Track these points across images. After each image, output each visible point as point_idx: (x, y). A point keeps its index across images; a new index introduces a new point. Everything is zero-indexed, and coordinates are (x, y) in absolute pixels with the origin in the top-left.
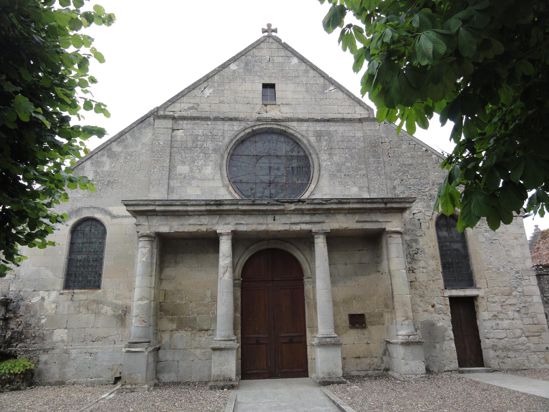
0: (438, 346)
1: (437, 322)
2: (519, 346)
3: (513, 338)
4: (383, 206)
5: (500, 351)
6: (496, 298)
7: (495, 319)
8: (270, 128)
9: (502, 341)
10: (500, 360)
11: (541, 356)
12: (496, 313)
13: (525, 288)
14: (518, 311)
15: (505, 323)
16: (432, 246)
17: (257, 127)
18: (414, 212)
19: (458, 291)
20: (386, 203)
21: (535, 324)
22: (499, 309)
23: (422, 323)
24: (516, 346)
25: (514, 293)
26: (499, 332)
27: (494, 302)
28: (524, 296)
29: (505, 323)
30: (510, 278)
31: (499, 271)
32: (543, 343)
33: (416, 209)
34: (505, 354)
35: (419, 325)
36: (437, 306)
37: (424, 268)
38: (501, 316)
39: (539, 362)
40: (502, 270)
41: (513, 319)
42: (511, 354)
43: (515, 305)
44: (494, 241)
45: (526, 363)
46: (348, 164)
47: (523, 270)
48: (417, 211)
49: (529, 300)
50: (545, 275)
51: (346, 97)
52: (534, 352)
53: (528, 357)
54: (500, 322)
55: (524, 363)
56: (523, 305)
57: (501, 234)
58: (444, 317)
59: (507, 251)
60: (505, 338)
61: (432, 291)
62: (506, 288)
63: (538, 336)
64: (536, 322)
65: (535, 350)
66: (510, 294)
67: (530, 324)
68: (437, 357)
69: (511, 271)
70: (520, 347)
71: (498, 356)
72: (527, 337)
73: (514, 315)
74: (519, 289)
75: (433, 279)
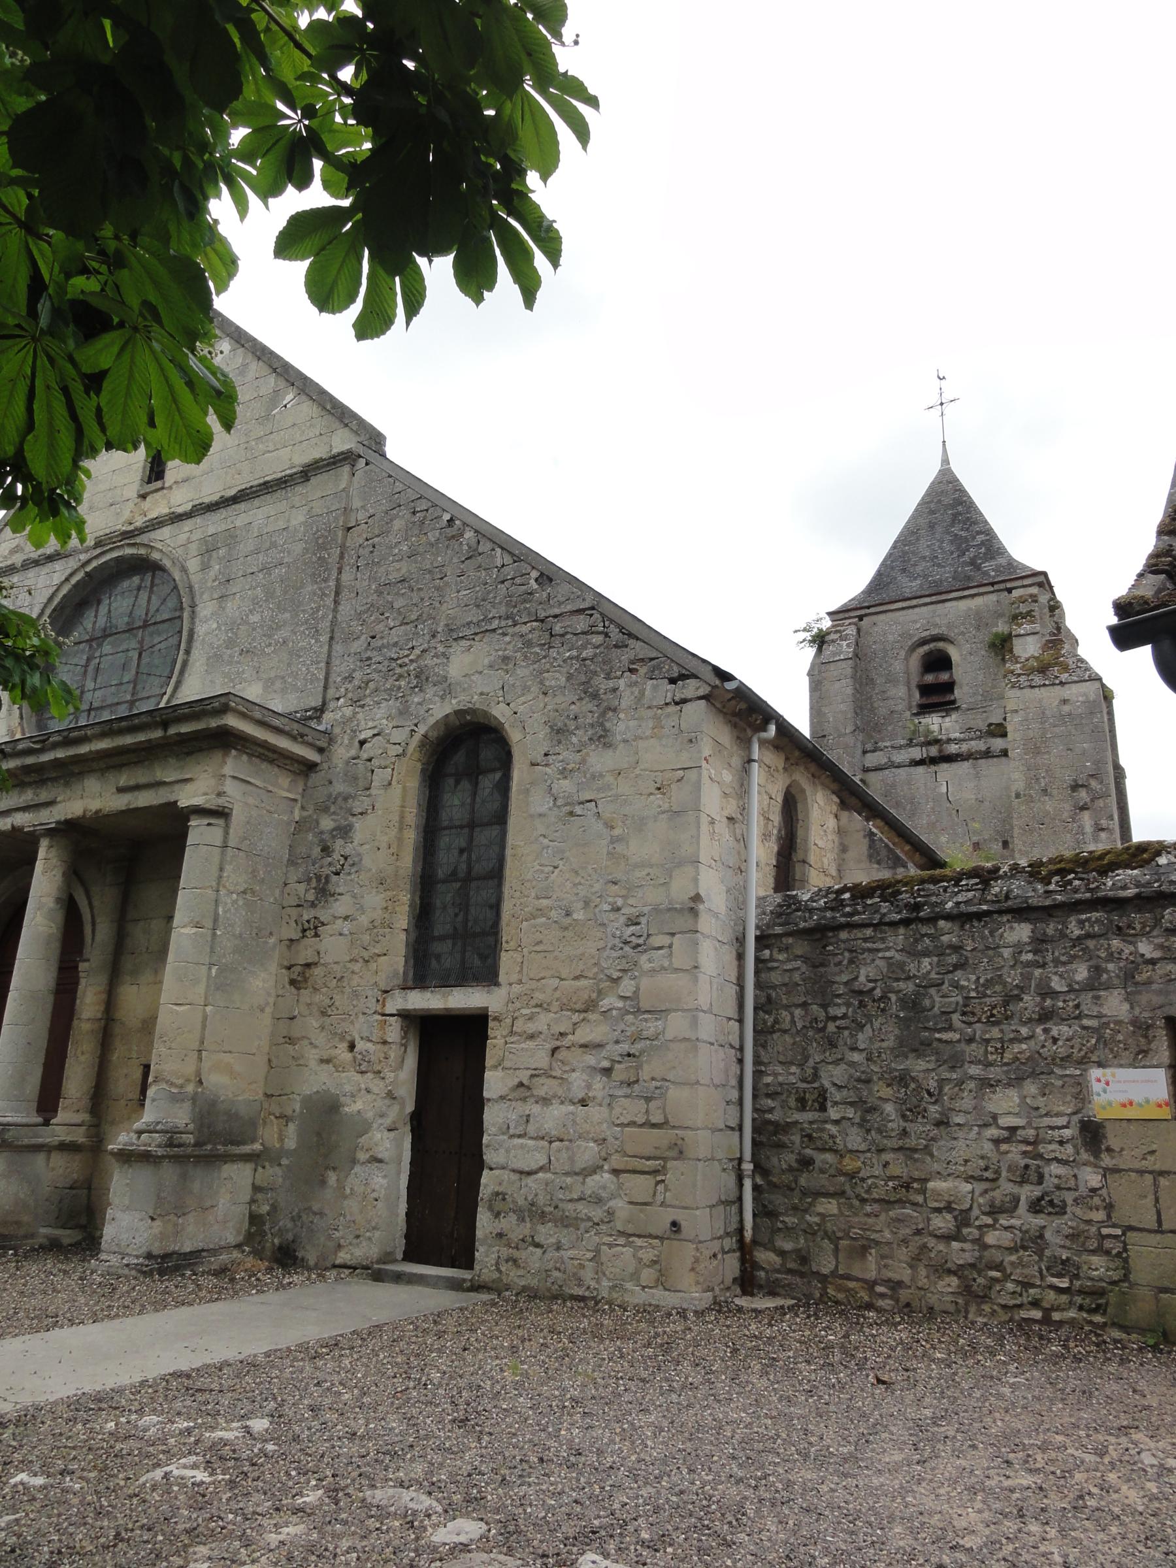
0: (332, 1178)
1: (348, 1100)
2: (580, 1206)
3: (567, 1174)
4: (158, 734)
5: (513, 1218)
6: (542, 1022)
7: (524, 1099)
8: (117, 560)
9: (530, 1181)
10: (505, 1252)
11: (648, 1255)
12: (524, 1076)
13: (645, 982)
14: (607, 1071)
15: (552, 1117)
16: (384, 845)
17: (94, 564)
18: (362, 736)
19: (428, 994)
20: (165, 725)
21: (654, 1126)
22: (541, 1059)
23: (307, 1101)
24: (570, 1206)
25: (605, 1003)
26: (522, 1146)
27: (532, 1037)
28: (639, 1011)
29: (552, 1117)
30: (601, 944)
31: (568, 920)
32: (663, 1204)
33: (370, 724)
34: (525, 1229)
35: (297, 1107)
36: (360, 1046)
37: (346, 918)
38: (544, 1087)
39: (635, 1276)
40: (579, 915)
41: (583, 1103)
42: (546, 1233)
43: (600, 1046)
44: (578, 810)
45: (588, 1275)
46: (255, 618)
47: (656, 910)
48: (370, 733)
49: (651, 1027)
50: (842, 927)
51: (315, 410)
52: (621, 1233)
53: (597, 1251)
54: (536, 1109)
55: (582, 1273)
56: (625, 1047)
57: (610, 779)
58: (371, 1086)
59: (614, 840)
60: (541, 1169)
61: (355, 994)
62: (583, 983)
63: (655, 1172)
64: (656, 1118)
65: (630, 1229)
66: (590, 1006)
67: (632, 1124)
68: (321, 1214)
69: (612, 916)
70: (583, 1209)
71: (500, 1235)
72: (616, 1172)
73: (589, 1087)
74: (627, 987)
75: (366, 955)
